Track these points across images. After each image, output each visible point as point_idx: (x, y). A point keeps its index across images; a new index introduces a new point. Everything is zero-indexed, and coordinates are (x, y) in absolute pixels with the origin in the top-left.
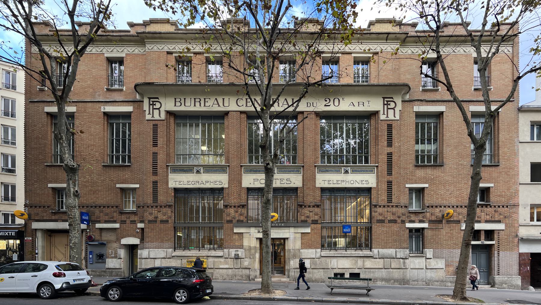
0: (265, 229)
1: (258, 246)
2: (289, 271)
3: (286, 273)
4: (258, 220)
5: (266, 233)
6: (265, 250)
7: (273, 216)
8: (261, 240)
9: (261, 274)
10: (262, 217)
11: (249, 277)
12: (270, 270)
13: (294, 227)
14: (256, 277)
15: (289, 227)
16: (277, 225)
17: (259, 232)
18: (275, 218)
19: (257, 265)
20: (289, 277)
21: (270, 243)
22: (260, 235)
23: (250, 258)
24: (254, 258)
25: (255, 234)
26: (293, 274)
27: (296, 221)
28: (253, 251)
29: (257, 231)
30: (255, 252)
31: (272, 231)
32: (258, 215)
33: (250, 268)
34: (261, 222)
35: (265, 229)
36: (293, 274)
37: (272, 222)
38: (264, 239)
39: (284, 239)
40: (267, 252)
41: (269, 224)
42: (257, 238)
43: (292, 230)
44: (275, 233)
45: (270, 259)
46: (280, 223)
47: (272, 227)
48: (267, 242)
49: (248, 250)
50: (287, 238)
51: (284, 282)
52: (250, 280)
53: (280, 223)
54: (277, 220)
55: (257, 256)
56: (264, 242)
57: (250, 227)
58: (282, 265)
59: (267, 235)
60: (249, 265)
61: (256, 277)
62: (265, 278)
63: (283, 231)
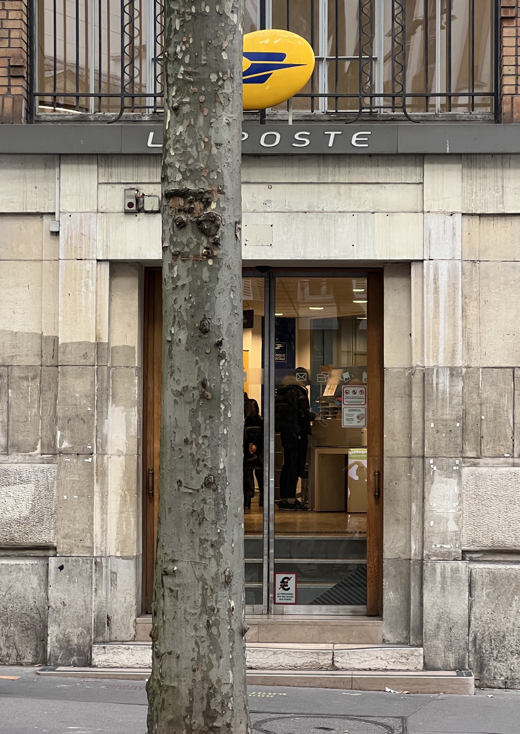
0: (191, 173)
1: (126, 333)
2: (416, 570)
3: (391, 597)
4: (130, 95)
5: (195, 216)
6: (182, 370)
7: (265, 65)
8: (149, 278)
9: (147, 605)
10: (166, 60)
11: (36, 628)
12: (233, 558)
13: (467, 159)
14: (102, 629)
15: (420, 159)
16: (302, 140)
17: (135, 207)
18: (282, 83)
19: (113, 523)
20: (413, 632)
21: (228, 300)
22: (145, 240)
23: (53, 452)
24: (88, 450)
25: (97, 227)
26: (457, 605)
27: (484, 111)
28: (77, 387)
29: (115, 198)
30: (102, 398)
31: (251, 196)
32: (131, 54)
33: (44, 550)
34: (158, 118)
35: (191, 173)
36: (457, 605)
37: (257, 117)
38: (175, 273)
39: (375, 274)
40: (207, 397)
41: (228, 131)
42: (117, 267)
43: (447, 187)
44: (283, 220)
45: (230, 460)
46: (336, 119)
47: (252, 157)
48: (202, 295)
49: (34, 373)
50: (403, 268)
51: (369, 684)
52: (43, 660)
53: (336, 119)
54: (309, 94)
55: (120, 428)
56: (175, 301)
57: (56, 159)
58: (354, 523)
59: (208, 228)
60: (37, 517)
61: (102, 629)
62: (185, 641)
63: (365, 196)
